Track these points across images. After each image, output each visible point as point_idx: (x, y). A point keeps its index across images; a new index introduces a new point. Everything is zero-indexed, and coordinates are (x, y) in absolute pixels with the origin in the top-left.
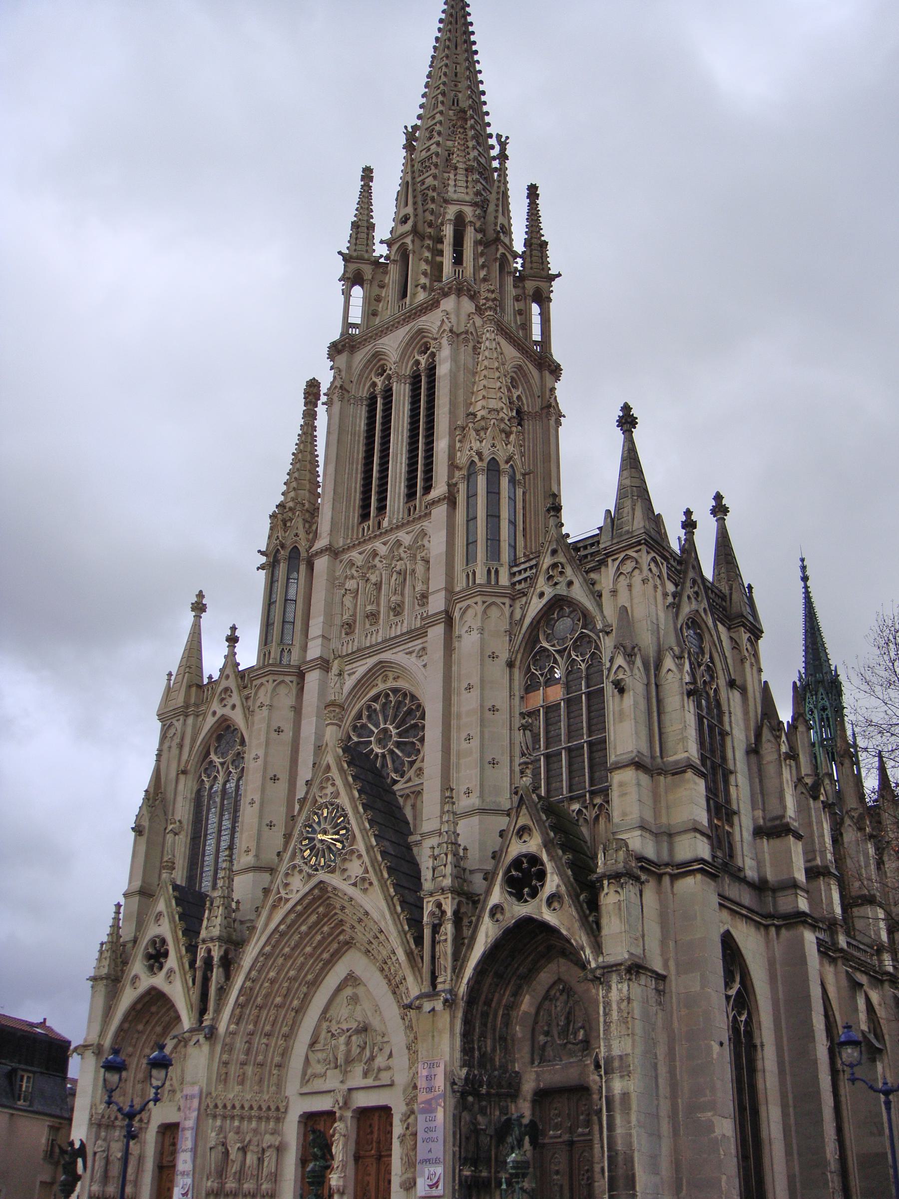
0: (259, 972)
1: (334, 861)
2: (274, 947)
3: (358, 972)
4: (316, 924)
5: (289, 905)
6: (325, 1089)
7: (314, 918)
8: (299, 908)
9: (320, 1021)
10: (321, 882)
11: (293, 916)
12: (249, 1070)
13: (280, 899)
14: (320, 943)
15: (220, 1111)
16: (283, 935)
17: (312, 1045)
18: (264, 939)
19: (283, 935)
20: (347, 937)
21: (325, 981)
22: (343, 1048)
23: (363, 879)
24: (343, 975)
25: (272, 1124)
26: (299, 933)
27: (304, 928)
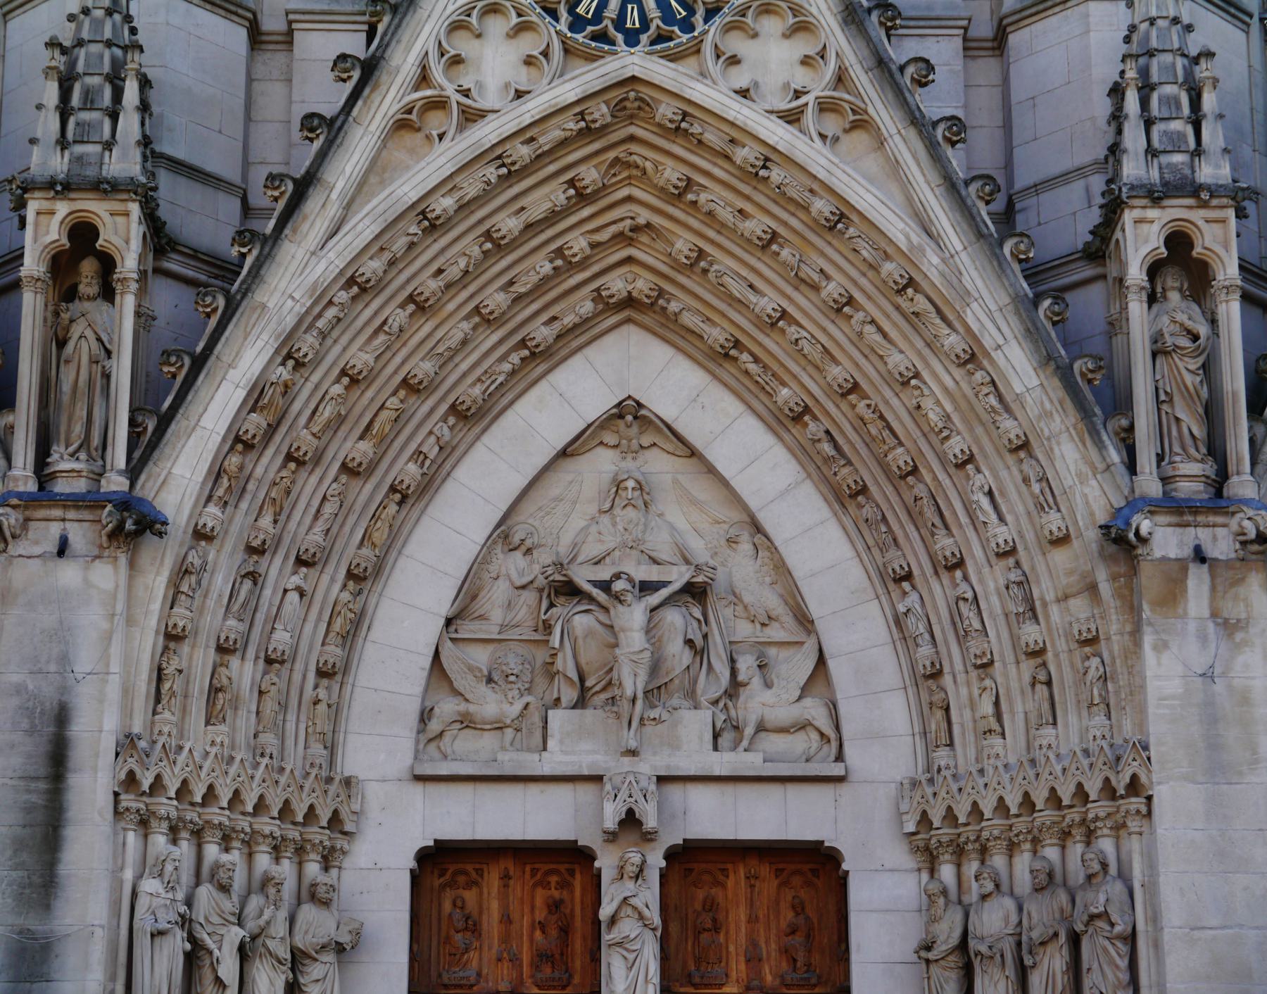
0: (323, 335)
1: (688, 26)
2: (392, 263)
3: (662, 405)
4: (554, 216)
5: (486, 133)
6: (547, 770)
7: (557, 194)
8: (523, 152)
9: (489, 544)
10: (634, 79)
11: (492, 173)
12: (244, 672)
13: (439, 104)
14: (543, 284)
15: (166, 806)
16: (433, 226)
17: (449, 622)
18: (362, 228)
19: (433, 226)
20: (642, 285)
21: (510, 416)
22: (634, 639)
23: (825, 107)
24: (597, 404)
25: (313, 869)
26: (488, 235)
27: (509, 224)
